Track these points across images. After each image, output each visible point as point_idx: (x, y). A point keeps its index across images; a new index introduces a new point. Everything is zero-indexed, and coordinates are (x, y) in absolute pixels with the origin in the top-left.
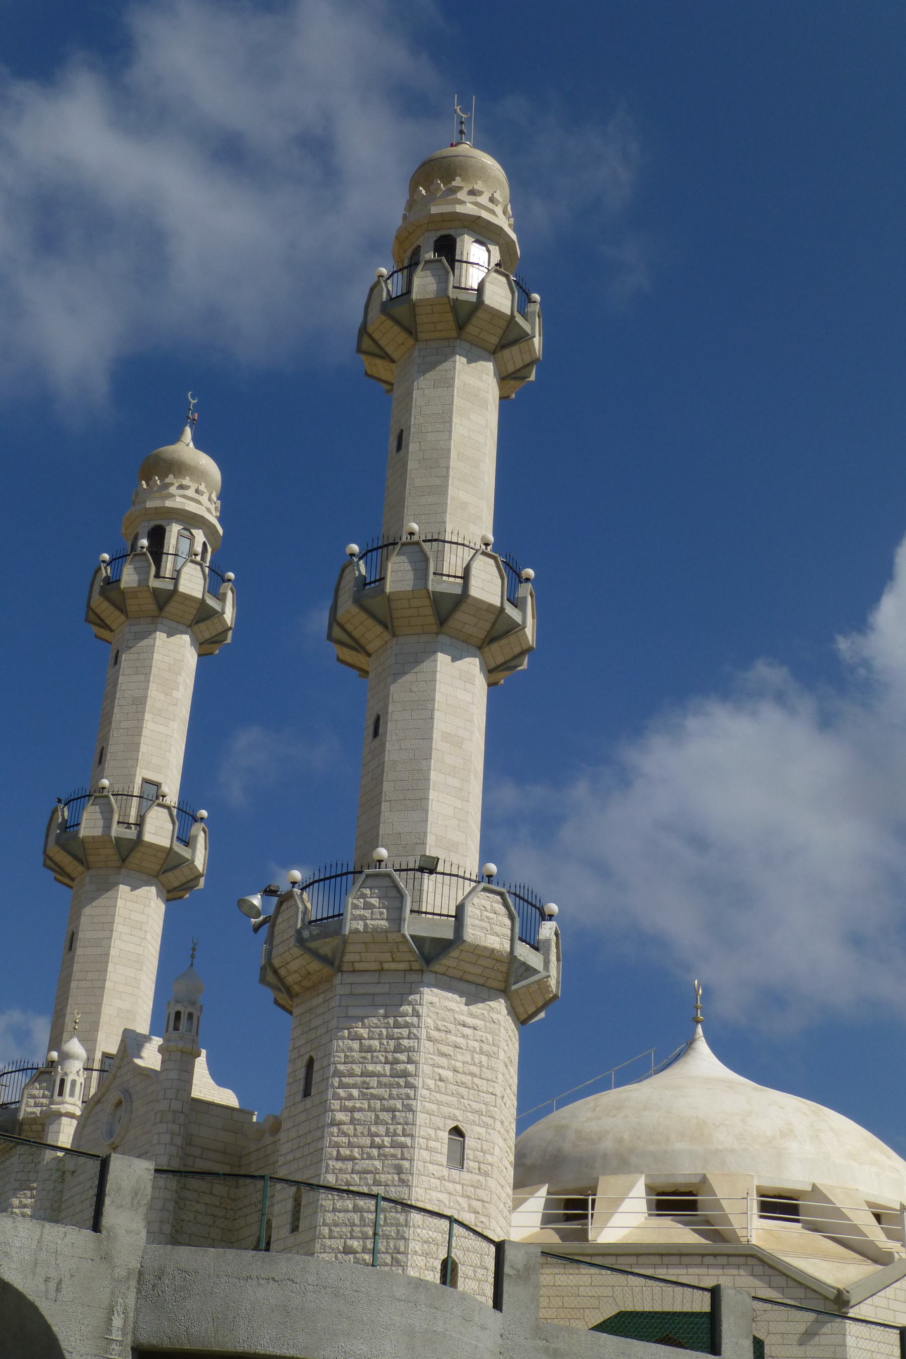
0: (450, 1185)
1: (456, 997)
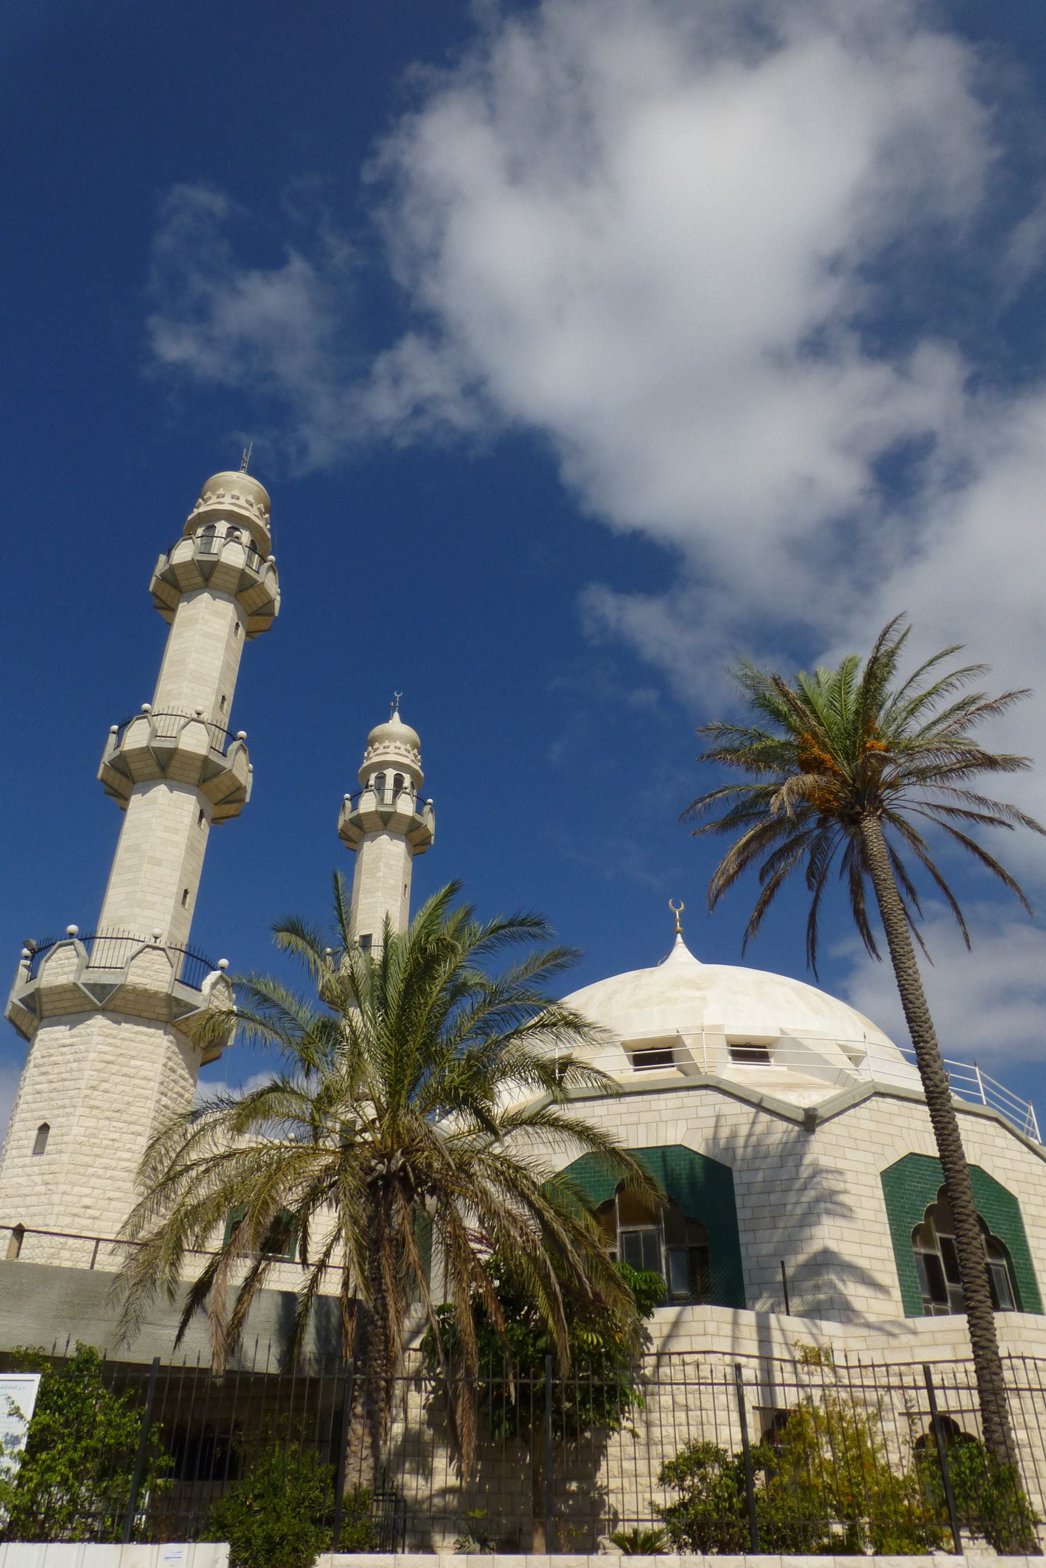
1: (63, 1028)
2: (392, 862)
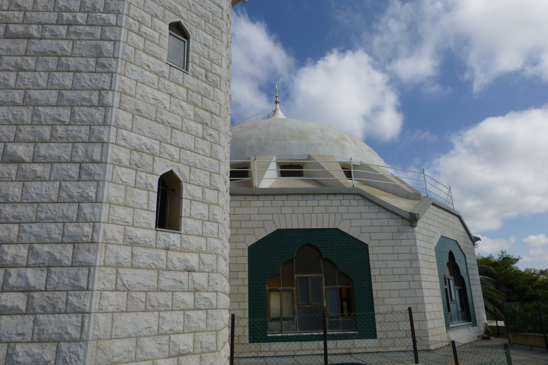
0: (172, 85)
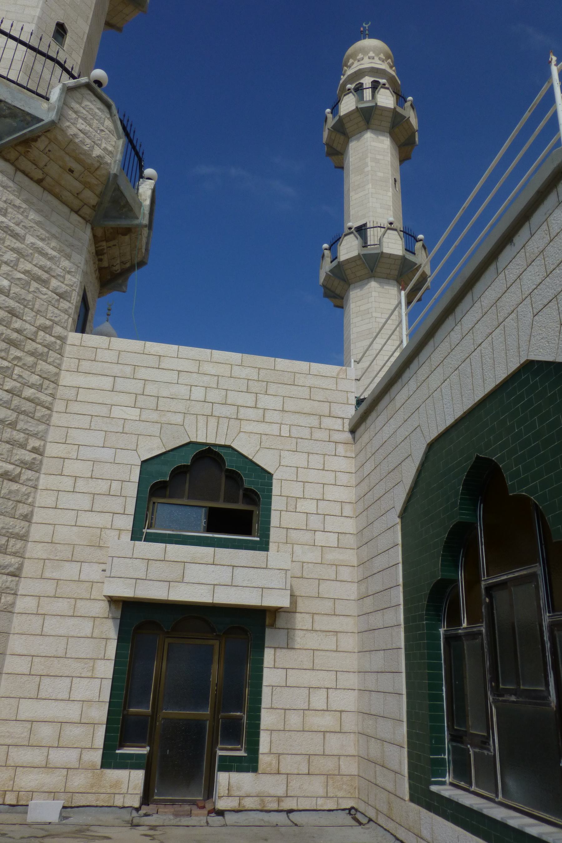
2: (378, 157)
